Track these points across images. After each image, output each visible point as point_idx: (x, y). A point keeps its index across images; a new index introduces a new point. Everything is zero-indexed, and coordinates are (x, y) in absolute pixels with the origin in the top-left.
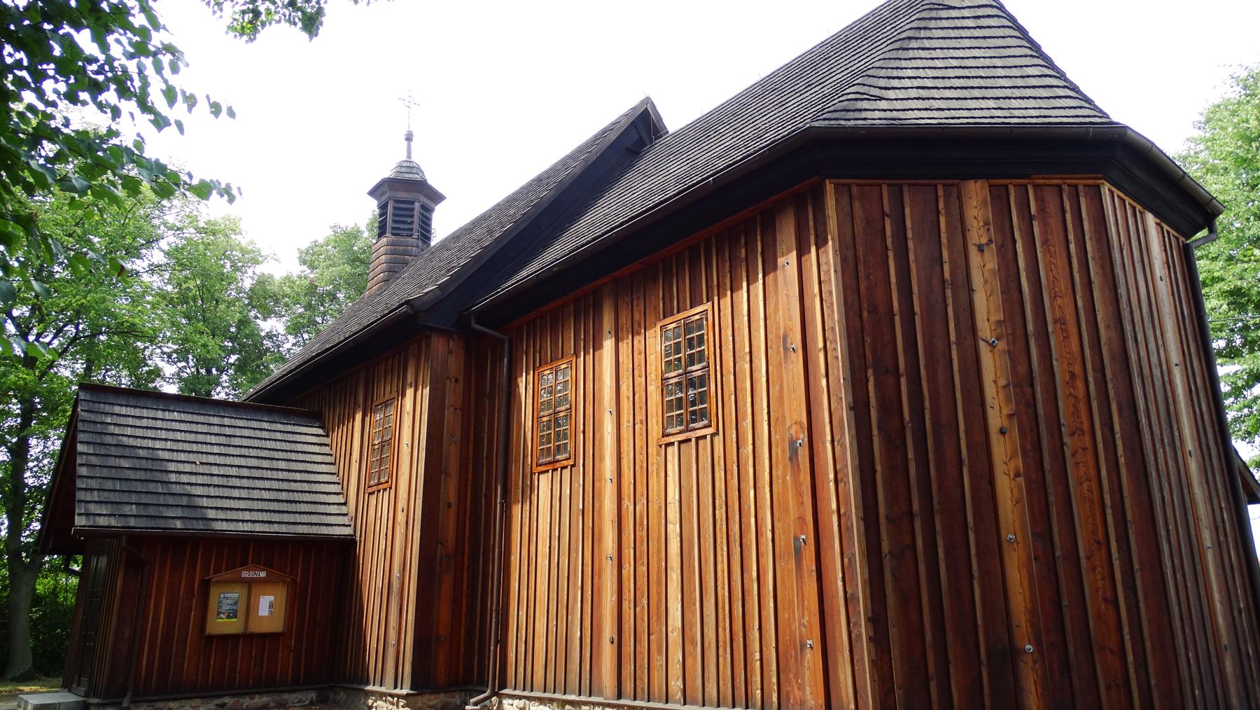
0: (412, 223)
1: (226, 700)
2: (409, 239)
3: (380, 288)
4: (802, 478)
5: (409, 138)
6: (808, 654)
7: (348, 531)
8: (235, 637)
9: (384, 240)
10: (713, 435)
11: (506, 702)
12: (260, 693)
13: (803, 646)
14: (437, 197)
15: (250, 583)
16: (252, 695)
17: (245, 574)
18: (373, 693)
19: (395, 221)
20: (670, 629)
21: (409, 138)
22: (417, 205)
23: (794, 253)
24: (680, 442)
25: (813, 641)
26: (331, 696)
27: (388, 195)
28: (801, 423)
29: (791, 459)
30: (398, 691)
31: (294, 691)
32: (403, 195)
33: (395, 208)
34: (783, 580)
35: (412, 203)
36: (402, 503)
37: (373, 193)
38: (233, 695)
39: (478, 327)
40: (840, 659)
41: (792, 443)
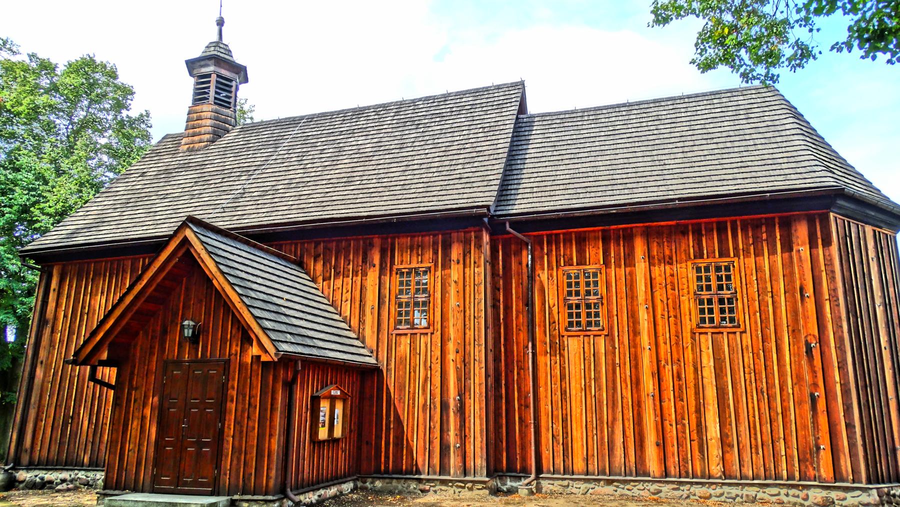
0: (230, 97)
1: (322, 492)
2: (228, 111)
3: (206, 146)
4: (815, 362)
5: (221, 23)
6: (822, 453)
7: (372, 361)
8: (324, 441)
9: (207, 109)
10: (741, 333)
11: (542, 482)
12: (333, 485)
13: (818, 448)
14: (246, 80)
15: (333, 399)
16: (329, 486)
17: (333, 393)
18: (428, 480)
19: (216, 93)
20: (709, 438)
21: (221, 23)
22: (234, 84)
23: (808, 246)
24: (713, 333)
25: (825, 445)
26: (359, 484)
27: (211, 69)
28: (814, 336)
29: (807, 352)
30: (467, 478)
31: (344, 483)
32: (224, 72)
33: (217, 82)
34: (801, 416)
35: (231, 81)
36: (451, 346)
37: (191, 65)
38: (324, 488)
39: (511, 230)
40: (842, 456)
41: (808, 345)
